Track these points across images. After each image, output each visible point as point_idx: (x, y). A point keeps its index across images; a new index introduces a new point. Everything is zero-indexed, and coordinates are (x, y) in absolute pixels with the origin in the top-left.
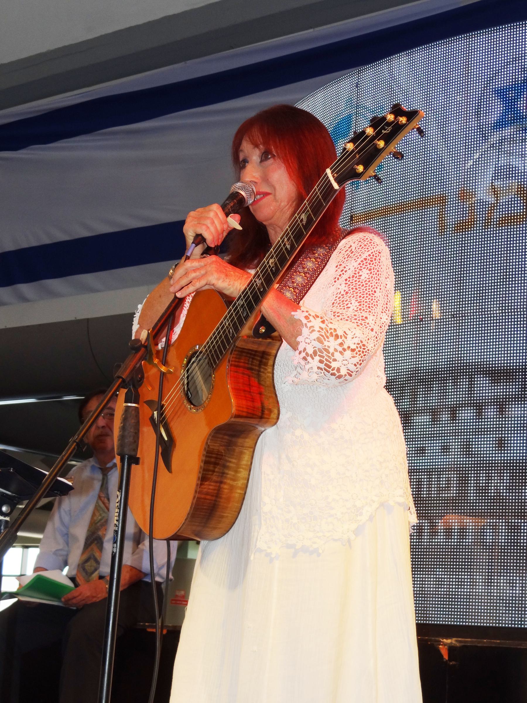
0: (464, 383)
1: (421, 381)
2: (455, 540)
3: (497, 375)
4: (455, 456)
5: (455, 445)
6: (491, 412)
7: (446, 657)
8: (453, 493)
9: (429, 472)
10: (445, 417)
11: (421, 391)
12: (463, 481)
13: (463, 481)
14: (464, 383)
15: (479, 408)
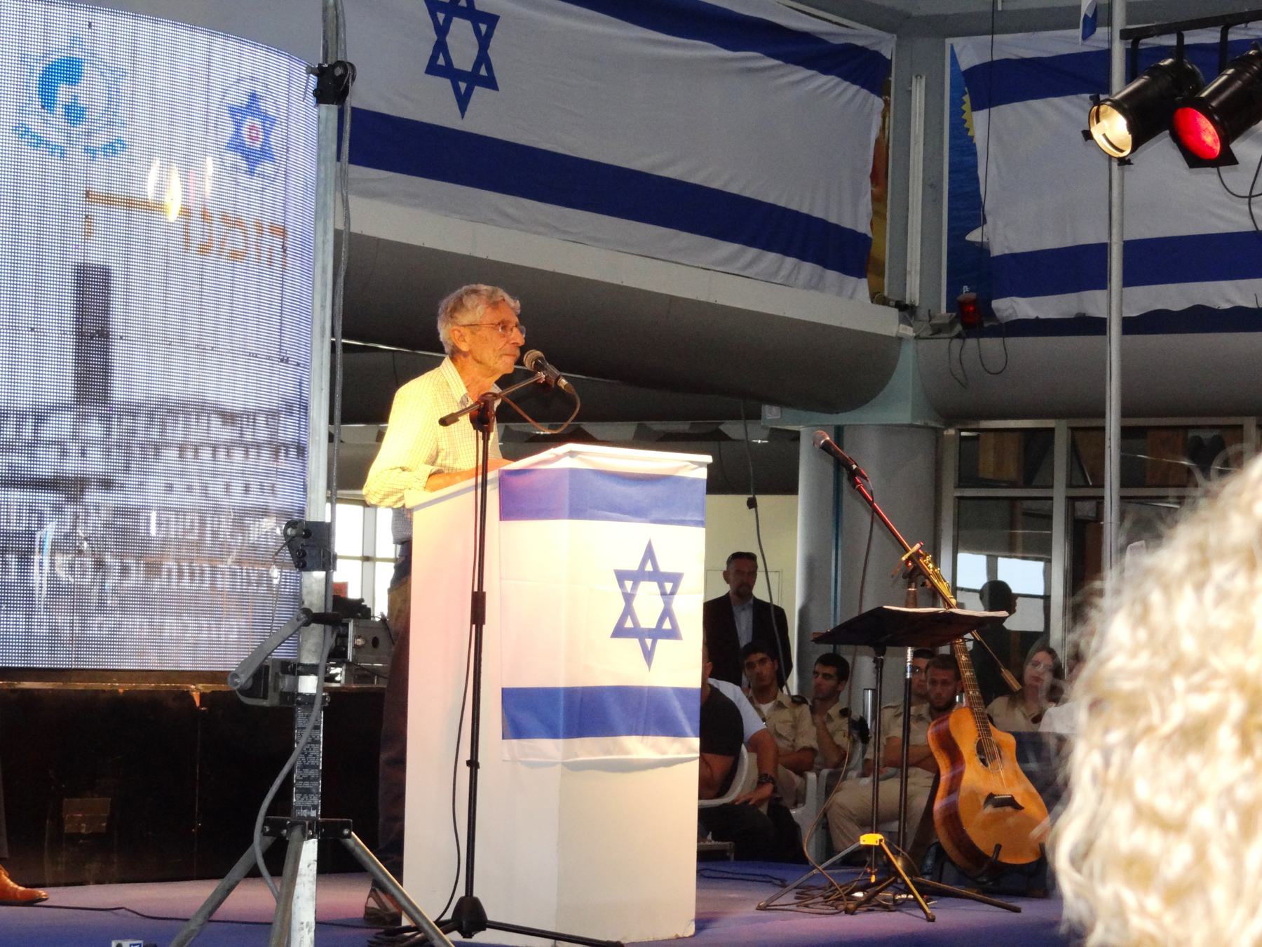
1: (170, 411)
2: (196, 585)
3: (228, 417)
6: (222, 454)
7: (198, 704)
9: (178, 511)
10: (190, 454)
11: (170, 422)
12: (202, 523)
13: (202, 523)
14: (204, 419)
15: (215, 449)
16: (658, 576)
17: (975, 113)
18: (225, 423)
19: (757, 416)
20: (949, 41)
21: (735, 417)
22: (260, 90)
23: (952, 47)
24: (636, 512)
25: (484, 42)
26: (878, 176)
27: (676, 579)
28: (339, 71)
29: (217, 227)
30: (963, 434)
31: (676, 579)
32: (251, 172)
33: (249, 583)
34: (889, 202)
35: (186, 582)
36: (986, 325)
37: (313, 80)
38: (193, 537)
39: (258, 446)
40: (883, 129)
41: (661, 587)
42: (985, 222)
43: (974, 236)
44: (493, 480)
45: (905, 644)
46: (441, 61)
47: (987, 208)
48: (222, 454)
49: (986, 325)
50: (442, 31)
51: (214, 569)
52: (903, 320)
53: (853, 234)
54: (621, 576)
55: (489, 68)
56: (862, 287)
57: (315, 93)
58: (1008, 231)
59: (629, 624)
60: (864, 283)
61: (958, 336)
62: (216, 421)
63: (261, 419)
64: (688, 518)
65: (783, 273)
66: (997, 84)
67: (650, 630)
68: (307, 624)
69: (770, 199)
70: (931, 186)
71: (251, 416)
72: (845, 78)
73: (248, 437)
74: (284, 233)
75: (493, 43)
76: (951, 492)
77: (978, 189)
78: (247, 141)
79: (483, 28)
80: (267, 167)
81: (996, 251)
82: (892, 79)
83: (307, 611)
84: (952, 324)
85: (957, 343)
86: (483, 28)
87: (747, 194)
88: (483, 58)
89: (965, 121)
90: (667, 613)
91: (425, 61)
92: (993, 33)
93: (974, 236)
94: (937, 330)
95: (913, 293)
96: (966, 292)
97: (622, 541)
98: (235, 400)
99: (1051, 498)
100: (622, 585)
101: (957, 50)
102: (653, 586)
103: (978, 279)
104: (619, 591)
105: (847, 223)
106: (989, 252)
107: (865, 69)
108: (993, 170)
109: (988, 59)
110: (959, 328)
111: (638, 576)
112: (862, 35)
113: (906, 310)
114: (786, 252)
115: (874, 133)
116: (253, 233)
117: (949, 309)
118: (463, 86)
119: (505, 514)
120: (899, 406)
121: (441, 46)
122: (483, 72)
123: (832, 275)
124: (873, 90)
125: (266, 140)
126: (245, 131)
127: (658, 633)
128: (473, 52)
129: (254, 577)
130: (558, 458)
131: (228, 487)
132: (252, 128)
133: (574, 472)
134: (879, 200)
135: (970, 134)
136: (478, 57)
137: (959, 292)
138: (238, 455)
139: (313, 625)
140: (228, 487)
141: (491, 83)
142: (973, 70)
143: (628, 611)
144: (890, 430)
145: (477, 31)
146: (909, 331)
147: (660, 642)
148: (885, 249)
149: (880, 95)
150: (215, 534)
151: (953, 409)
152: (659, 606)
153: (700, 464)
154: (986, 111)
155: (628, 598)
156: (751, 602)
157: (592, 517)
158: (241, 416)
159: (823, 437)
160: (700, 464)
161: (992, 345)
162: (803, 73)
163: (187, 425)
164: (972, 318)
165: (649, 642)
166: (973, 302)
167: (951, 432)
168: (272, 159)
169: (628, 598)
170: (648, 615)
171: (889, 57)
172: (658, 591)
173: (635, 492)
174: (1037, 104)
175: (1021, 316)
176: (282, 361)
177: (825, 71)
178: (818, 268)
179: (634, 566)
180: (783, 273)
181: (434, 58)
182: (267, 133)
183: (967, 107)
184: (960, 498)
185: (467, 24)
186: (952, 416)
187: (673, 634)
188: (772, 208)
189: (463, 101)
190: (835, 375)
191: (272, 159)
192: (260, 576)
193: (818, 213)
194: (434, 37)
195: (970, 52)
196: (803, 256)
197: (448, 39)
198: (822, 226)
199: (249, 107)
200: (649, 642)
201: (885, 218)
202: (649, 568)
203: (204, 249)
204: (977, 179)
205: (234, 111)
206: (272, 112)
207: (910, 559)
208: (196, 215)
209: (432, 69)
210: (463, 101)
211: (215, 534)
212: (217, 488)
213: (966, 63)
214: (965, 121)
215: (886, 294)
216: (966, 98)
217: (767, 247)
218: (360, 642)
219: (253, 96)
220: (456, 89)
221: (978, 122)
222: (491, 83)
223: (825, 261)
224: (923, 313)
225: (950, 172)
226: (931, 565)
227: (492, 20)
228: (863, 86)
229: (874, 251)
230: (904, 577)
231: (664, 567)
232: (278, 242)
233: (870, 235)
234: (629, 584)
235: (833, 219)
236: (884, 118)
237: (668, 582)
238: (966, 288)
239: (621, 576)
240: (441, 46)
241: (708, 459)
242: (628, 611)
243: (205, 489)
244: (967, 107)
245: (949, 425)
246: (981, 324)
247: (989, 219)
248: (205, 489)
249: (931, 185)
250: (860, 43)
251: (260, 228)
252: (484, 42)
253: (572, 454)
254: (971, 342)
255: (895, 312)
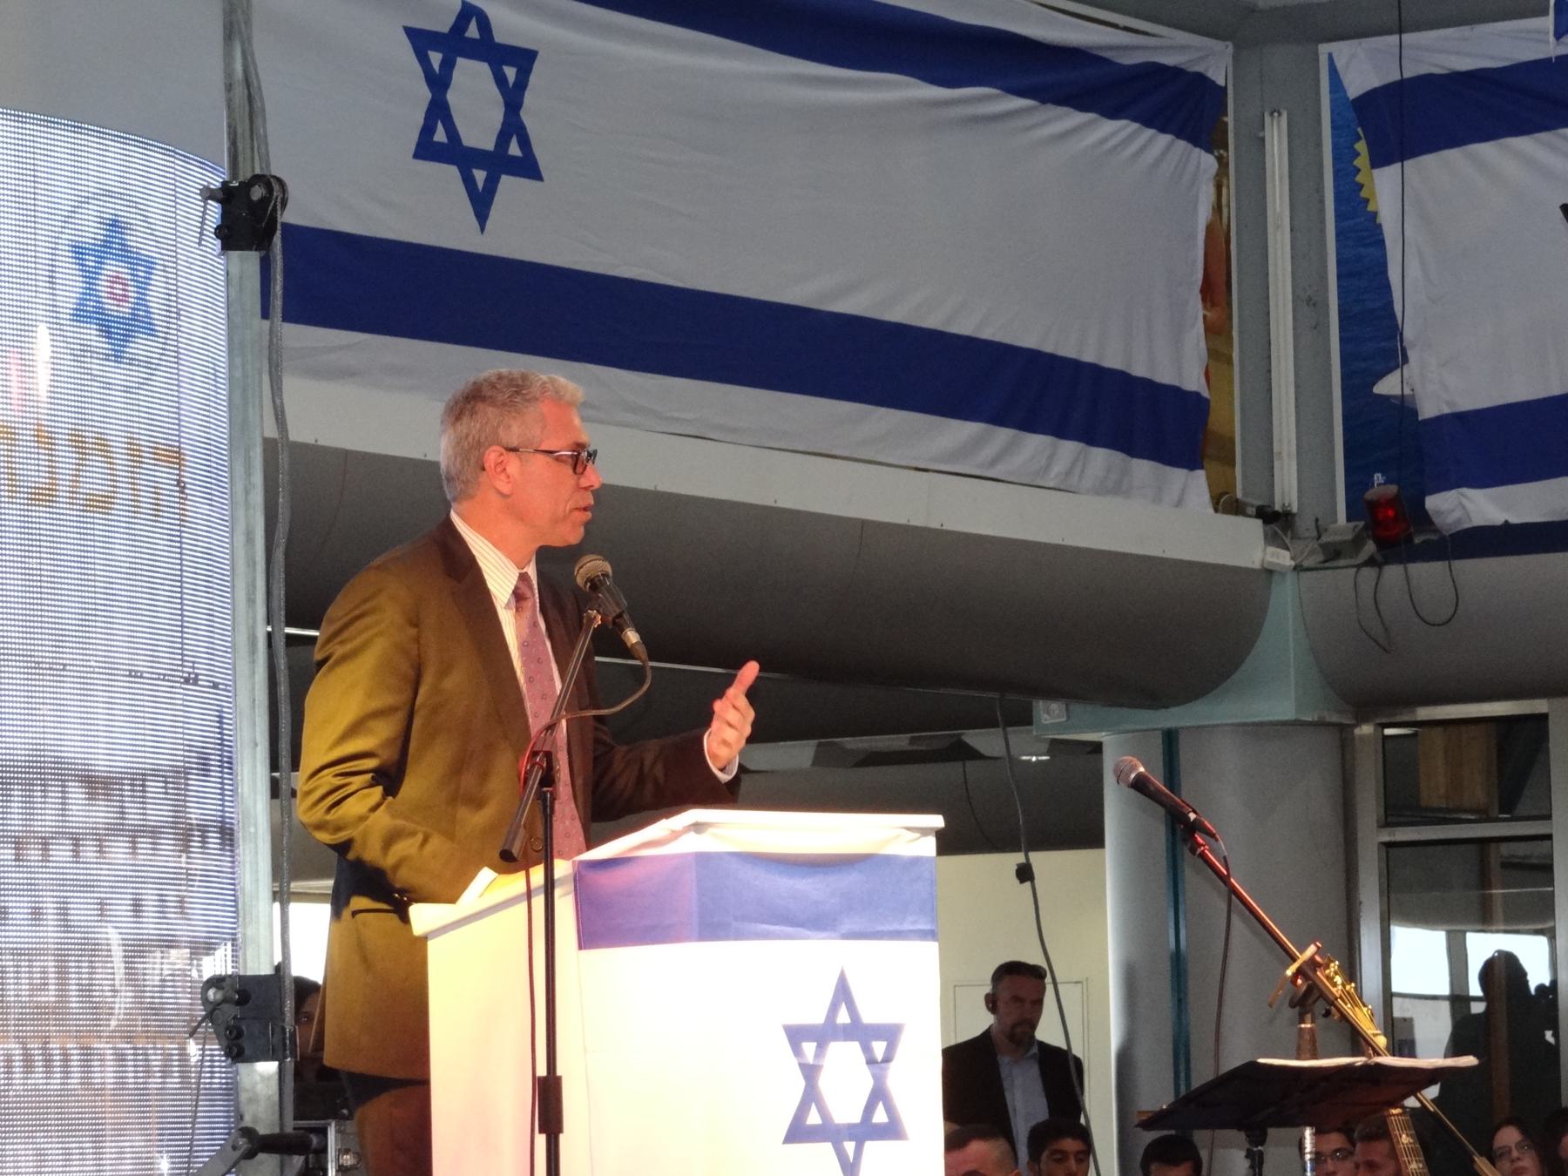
0: (54, 793)
2: (56, 1080)
3: (97, 785)
4: (50, 931)
5: (50, 907)
6: (89, 852)
8: (50, 996)
10: (34, 854)
12: (62, 973)
14: (54, 793)
15: (76, 841)
16: (860, 1032)
17: (1376, 172)
18: (92, 796)
19: (1024, 718)
20: (1324, 49)
21: (989, 723)
22: (125, 214)
23: (1330, 56)
24: (817, 921)
25: (513, 99)
26: (1214, 289)
27: (891, 1034)
28: (257, 193)
29: (66, 457)
30: (1389, 732)
31: (891, 1034)
32: (117, 357)
33: (148, 1072)
34: (1235, 334)
35: (38, 1078)
36: (1417, 540)
37: (215, 209)
38: (50, 996)
39: (154, 833)
40: (1218, 208)
41: (867, 1049)
42: (1405, 360)
43: (1388, 386)
44: (564, 880)
45: (1298, 1123)
46: (440, 136)
47: (1408, 333)
48: (89, 852)
49: (1417, 540)
50: (439, 82)
51: (87, 1052)
52: (1272, 539)
53: (1176, 391)
54: (796, 1035)
55: (525, 143)
56: (1195, 485)
57: (219, 232)
58: (1445, 375)
59: (813, 1118)
60: (1200, 475)
61: (1371, 562)
62: (76, 793)
63: (154, 787)
64: (906, 926)
65: (1058, 468)
66: (1412, 119)
67: (851, 1127)
68: (250, 1155)
69: (1029, 341)
70: (1307, 301)
71: (140, 780)
72: (1148, 122)
73: (133, 817)
74: (176, 457)
75: (529, 98)
76: (1371, 837)
77: (1391, 303)
78: (110, 305)
79: (510, 73)
80: (141, 346)
81: (1428, 410)
82: (1230, 119)
83: (248, 1133)
84: (1357, 543)
85: (1369, 573)
86: (510, 73)
87: (986, 334)
88: (513, 126)
89: (1362, 186)
90: (879, 1095)
91: (413, 137)
92: (1401, 31)
93: (1388, 386)
94: (1333, 553)
95: (1287, 490)
96: (1380, 485)
97: (791, 973)
98: (107, 752)
99: (1549, 837)
100: (797, 1051)
101: (1339, 64)
102: (854, 1048)
103: (1399, 461)
104: (794, 1062)
105: (1165, 376)
106: (1415, 413)
107: (1181, 106)
108: (1413, 270)
109: (1396, 77)
110: (1370, 547)
111: (824, 1034)
112: (1176, 48)
113: (1276, 521)
114: (1060, 432)
115: (1204, 214)
116: (121, 460)
117: (1349, 519)
118: (480, 176)
119: (588, 938)
120: (1277, 689)
121: (438, 110)
122: (514, 150)
123: (1143, 468)
124: (1196, 141)
125: (142, 299)
126: (103, 286)
127: (866, 1131)
128: (496, 115)
129: (156, 1062)
130: (675, 835)
131: (102, 906)
132: (116, 279)
133: (703, 859)
134: (1217, 331)
135: (1370, 208)
136: (504, 124)
137: (1369, 484)
138: (118, 852)
139: (261, 1156)
140: (102, 906)
141: (528, 168)
142: (1370, 99)
143: (811, 1095)
144: (1260, 731)
145: (500, 80)
146: (1282, 558)
147: (870, 1147)
148: (1231, 416)
149: (1209, 150)
150: (86, 991)
151: (1368, 687)
152: (864, 1082)
153: (924, 832)
154: (1395, 168)
155: (810, 1072)
156: (1035, 1050)
157: (739, 936)
158: (119, 781)
159: (1133, 768)
160: (924, 832)
161: (1428, 573)
162: (1075, 118)
163: (28, 804)
164: (1393, 530)
165: (850, 1147)
166: (1392, 502)
167: (1366, 729)
168: (150, 331)
169: (810, 1072)
170: (845, 1098)
171: (1221, 82)
172: (861, 1058)
173: (810, 887)
174: (1486, 150)
175: (1478, 521)
176: (187, 681)
177: (1113, 113)
178: (1117, 457)
179: (815, 1015)
180: (1058, 468)
181: (427, 130)
182: (143, 287)
183: (1362, 161)
184: (1389, 845)
185: (483, 69)
186: (1371, 702)
187: (892, 1131)
188: (1034, 356)
189: (482, 203)
190: (1160, 644)
191: (150, 331)
192: (167, 1058)
193: (1113, 361)
194: (425, 94)
195: (1363, 66)
196: (1090, 437)
197: (452, 97)
198: (1123, 381)
199: (106, 244)
200: (850, 1147)
201: (1229, 361)
202: (843, 1017)
203: (45, 495)
204: (1387, 287)
205: (79, 251)
206: (148, 249)
207: (1299, 972)
208: (27, 436)
209: (426, 150)
210: (482, 203)
211: (86, 991)
212: (82, 911)
213: (1356, 86)
214: (1362, 186)
215: (1239, 495)
216: (1361, 146)
217: (1029, 425)
218: (348, 1160)
219: (114, 224)
220: (469, 181)
221: (1384, 187)
222: (528, 168)
223: (1129, 445)
224: (1305, 525)
225: (1339, 277)
226: (1338, 979)
227: (524, 59)
228: (1179, 134)
229: (1215, 420)
230: (1292, 1005)
231: (869, 1017)
232: (166, 475)
233: (1205, 394)
234: (809, 1048)
235: (1139, 370)
236: (1219, 187)
237: (877, 1041)
238: (1378, 478)
239: (796, 1035)
240: (438, 110)
241: (937, 821)
242: (811, 1095)
243: (63, 911)
244: (1362, 161)
245: (1361, 719)
246: (1409, 539)
247: (1410, 353)
248: (63, 911)
249: (1309, 299)
250: (1169, 60)
251: (134, 451)
252: (513, 99)
253: (698, 827)
254: (1393, 572)
255: (1256, 525)
